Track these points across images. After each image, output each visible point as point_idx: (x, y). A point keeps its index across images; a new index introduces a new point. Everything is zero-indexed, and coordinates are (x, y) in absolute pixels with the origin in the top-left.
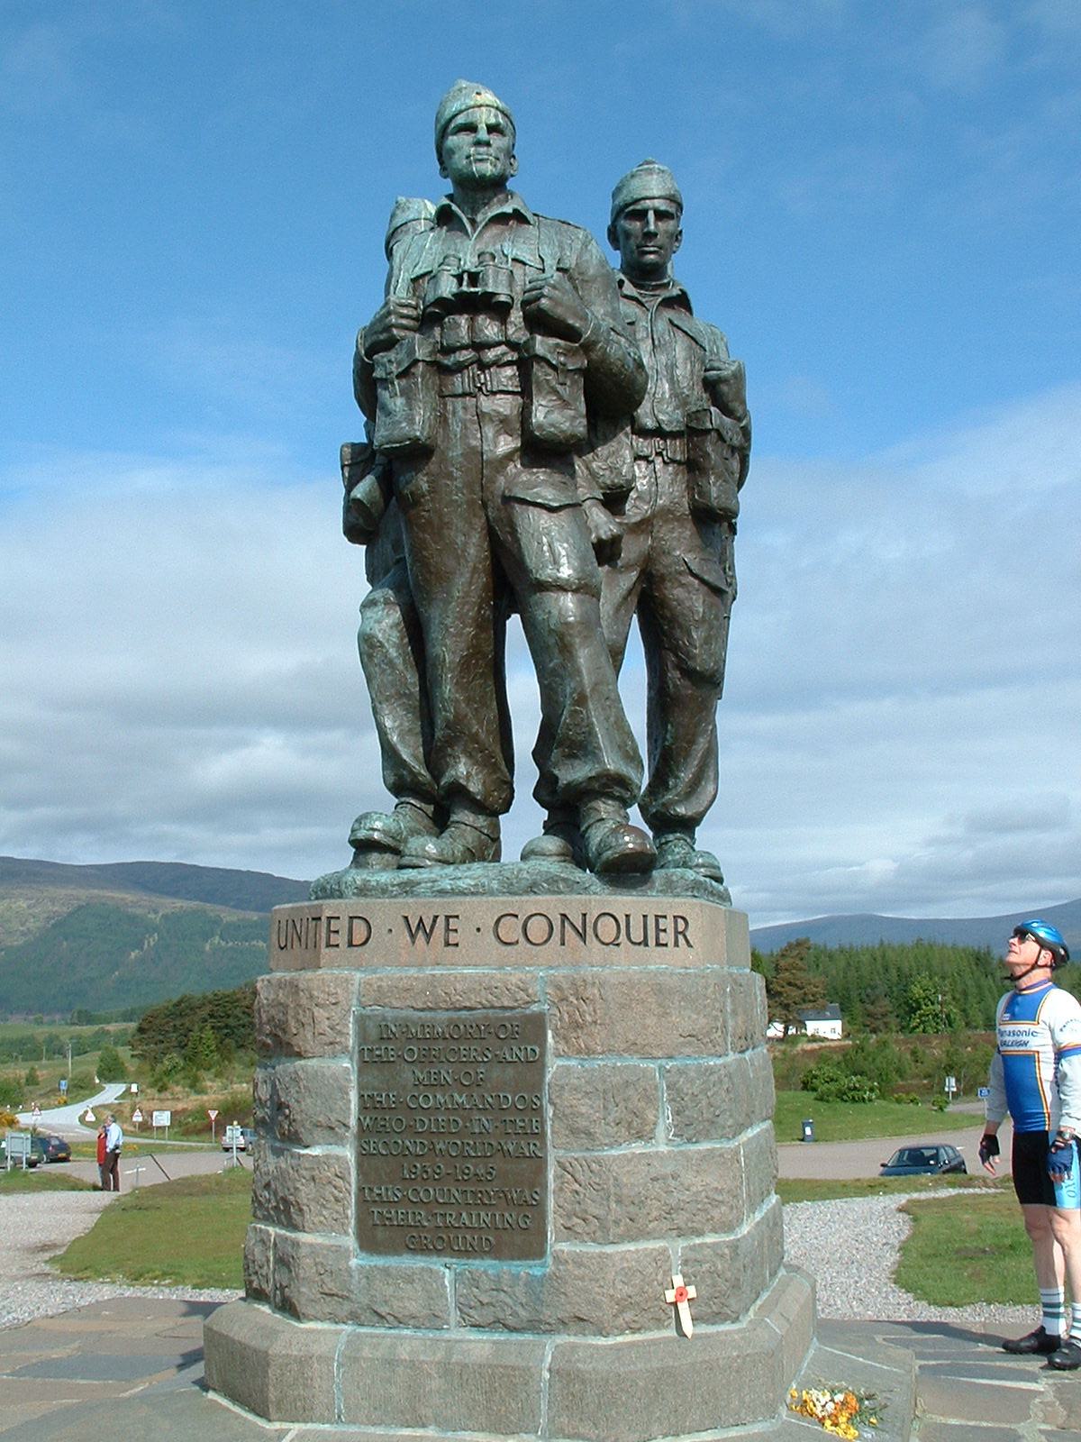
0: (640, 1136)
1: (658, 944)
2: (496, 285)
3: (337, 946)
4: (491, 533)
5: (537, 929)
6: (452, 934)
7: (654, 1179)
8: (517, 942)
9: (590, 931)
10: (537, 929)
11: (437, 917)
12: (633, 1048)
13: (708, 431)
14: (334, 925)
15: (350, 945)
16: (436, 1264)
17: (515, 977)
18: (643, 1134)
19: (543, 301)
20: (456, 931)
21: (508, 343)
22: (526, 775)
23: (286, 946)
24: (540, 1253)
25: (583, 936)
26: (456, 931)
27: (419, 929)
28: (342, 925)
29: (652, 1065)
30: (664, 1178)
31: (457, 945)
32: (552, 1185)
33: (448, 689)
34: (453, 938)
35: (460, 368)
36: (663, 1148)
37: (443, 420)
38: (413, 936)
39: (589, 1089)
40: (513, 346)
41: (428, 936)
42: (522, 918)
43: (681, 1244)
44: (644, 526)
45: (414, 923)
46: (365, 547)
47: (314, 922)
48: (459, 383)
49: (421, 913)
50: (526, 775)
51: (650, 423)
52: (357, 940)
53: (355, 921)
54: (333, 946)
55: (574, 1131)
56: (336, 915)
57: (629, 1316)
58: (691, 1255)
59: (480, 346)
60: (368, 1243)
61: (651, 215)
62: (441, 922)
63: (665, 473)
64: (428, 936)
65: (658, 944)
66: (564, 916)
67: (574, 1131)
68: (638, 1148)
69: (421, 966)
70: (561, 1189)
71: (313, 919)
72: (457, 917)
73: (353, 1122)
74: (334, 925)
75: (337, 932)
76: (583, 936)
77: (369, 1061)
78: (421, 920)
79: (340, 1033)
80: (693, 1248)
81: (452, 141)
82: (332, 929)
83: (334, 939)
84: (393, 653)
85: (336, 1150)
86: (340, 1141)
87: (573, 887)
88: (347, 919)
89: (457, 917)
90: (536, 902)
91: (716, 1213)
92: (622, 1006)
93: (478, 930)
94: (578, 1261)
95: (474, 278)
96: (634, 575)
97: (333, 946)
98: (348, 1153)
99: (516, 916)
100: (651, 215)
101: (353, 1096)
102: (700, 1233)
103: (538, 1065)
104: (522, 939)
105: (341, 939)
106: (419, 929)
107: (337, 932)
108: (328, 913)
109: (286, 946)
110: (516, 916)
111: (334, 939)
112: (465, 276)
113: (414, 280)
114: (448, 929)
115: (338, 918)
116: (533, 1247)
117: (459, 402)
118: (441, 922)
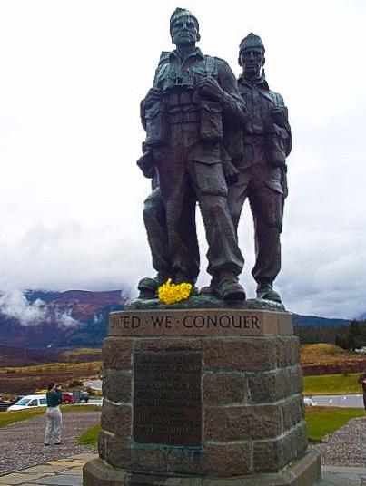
0: (236, 401)
1: (245, 327)
2: (189, 83)
4: (187, 173)
5: (199, 321)
6: (169, 325)
7: (243, 417)
9: (218, 322)
10: (199, 321)
12: (235, 367)
13: (272, 134)
15: (133, 327)
16: (161, 447)
18: (239, 400)
19: (205, 88)
21: (193, 103)
22: (204, 263)
24: (200, 445)
25: (215, 324)
27: (157, 321)
29: (243, 374)
30: (246, 416)
32: (203, 418)
33: (171, 233)
34: (169, 325)
35: (177, 113)
36: (247, 405)
37: (168, 133)
38: (155, 324)
40: (195, 105)
41: (160, 324)
43: (253, 442)
44: (248, 170)
46: (151, 179)
48: (175, 120)
50: (204, 263)
51: (251, 131)
55: (210, 398)
57: (233, 469)
58: (257, 446)
59: (182, 106)
60: (138, 439)
61: (252, 54)
63: (257, 150)
64: (160, 324)
65: (245, 327)
67: (210, 398)
68: (236, 405)
70: (206, 421)
73: (132, 393)
76: (215, 324)
77: (138, 370)
80: (258, 444)
84: (155, 219)
85: (127, 404)
86: (128, 400)
87: (215, 306)
91: (267, 430)
92: (229, 351)
94: (213, 448)
95: (180, 80)
96: (245, 186)
98: (131, 405)
100: (252, 54)
101: (132, 383)
102: (261, 438)
103: (199, 372)
105: (130, 325)
116: (197, 441)
117: (176, 126)
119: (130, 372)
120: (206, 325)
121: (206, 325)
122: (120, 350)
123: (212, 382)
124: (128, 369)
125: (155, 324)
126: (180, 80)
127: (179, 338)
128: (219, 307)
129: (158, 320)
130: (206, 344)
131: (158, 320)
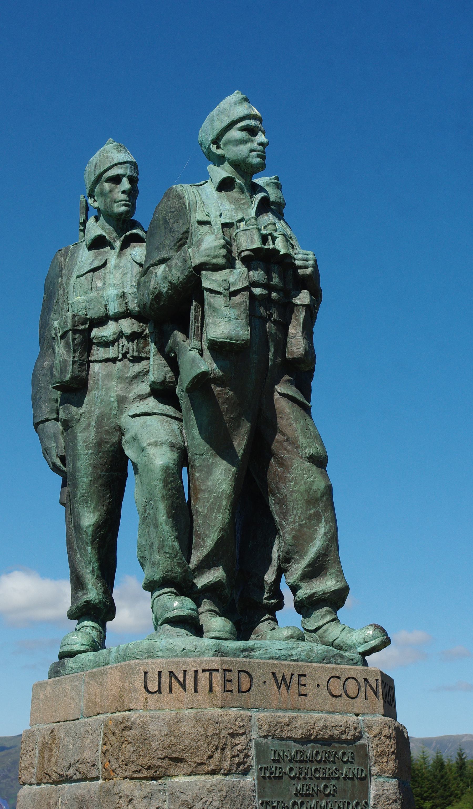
3: (231, 691)
6: (302, 688)
8: (340, 696)
11: (292, 675)
14: (229, 676)
17: (350, 719)
20: (305, 685)
23: (159, 691)
25: (376, 694)
26: (305, 685)
27: (282, 682)
28: (233, 676)
31: (306, 695)
34: (303, 690)
38: (279, 687)
39: (394, 797)
42: (343, 679)
45: (279, 678)
47: (207, 674)
49: (283, 671)
52: (245, 687)
53: (243, 674)
54: (228, 691)
56: (230, 668)
62: (295, 678)
66: (366, 680)
69: (285, 710)
71: (204, 671)
72: (305, 676)
74: (229, 676)
75: (230, 681)
78: (283, 675)
79: (247, 756)
81: (235, 134)
82: (227, 678)
83: (229, 686)
87: (351, 661)
88: (237, 673)
89: (305, 676)
90: (350, 670)
93: (318, 685)
97: (228, 691)
99: (339, 678)
104: (343, 694)
105: (234, 686)
106: (282, 682)
107: (230, 681)
108: (225, 667)
109: (159, 691)
110: (339, 678)
111: (229, 686)
112: (269, 237)
113: (225, 225)
114: (300, 684)
115: (230, 671)
118: (295, 678)
119: (249, 780)
120: (362, 694)
121: (362, 694)
122: (233, 735)
123: (388, 798)
124: (245, 773)
125: (279, 687)
126: (274, 239)
127: (321, 715)
128: (356, 664)
129: (283, 678)
130: (370, 727)
131: (283, 678)
